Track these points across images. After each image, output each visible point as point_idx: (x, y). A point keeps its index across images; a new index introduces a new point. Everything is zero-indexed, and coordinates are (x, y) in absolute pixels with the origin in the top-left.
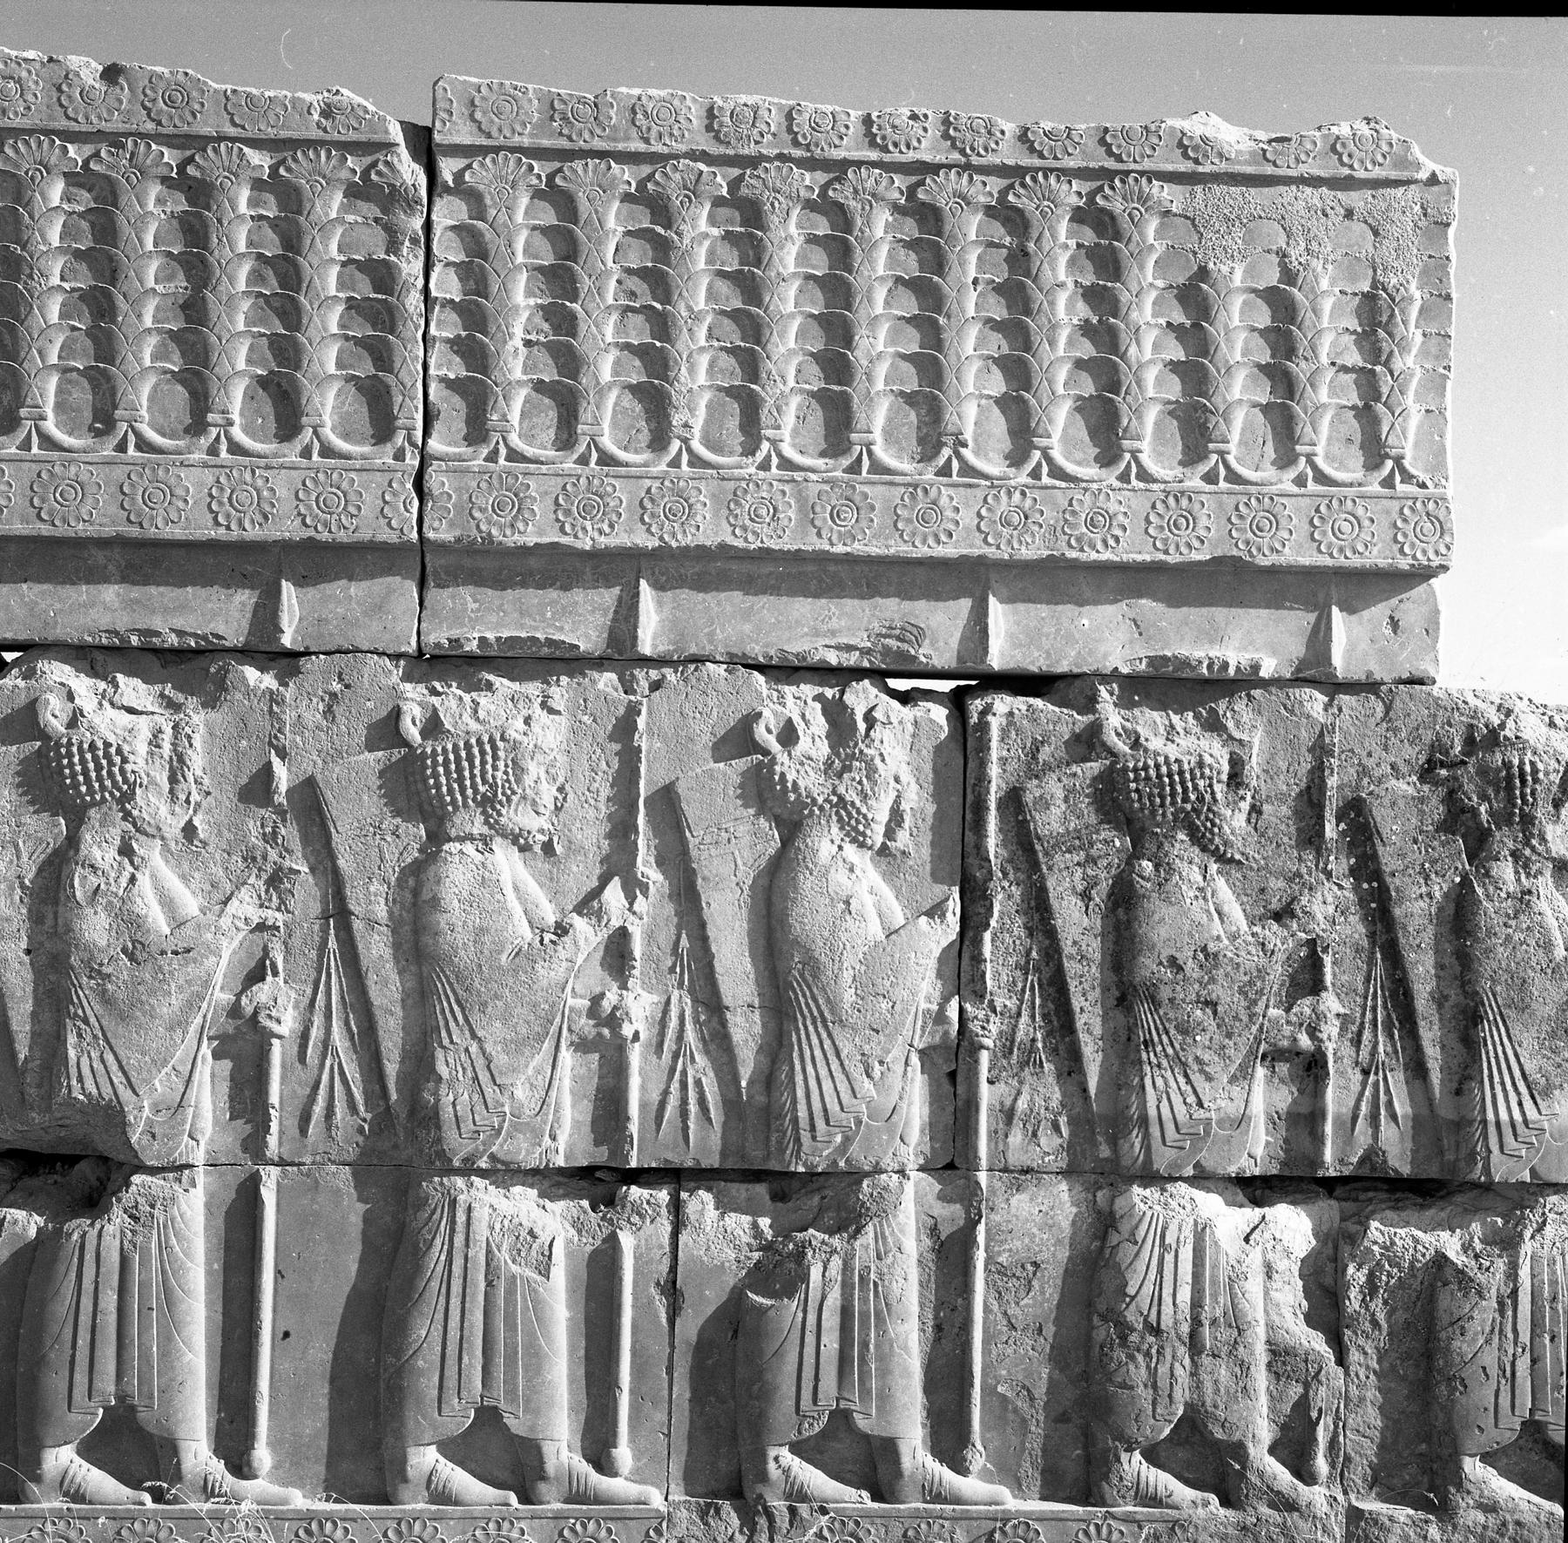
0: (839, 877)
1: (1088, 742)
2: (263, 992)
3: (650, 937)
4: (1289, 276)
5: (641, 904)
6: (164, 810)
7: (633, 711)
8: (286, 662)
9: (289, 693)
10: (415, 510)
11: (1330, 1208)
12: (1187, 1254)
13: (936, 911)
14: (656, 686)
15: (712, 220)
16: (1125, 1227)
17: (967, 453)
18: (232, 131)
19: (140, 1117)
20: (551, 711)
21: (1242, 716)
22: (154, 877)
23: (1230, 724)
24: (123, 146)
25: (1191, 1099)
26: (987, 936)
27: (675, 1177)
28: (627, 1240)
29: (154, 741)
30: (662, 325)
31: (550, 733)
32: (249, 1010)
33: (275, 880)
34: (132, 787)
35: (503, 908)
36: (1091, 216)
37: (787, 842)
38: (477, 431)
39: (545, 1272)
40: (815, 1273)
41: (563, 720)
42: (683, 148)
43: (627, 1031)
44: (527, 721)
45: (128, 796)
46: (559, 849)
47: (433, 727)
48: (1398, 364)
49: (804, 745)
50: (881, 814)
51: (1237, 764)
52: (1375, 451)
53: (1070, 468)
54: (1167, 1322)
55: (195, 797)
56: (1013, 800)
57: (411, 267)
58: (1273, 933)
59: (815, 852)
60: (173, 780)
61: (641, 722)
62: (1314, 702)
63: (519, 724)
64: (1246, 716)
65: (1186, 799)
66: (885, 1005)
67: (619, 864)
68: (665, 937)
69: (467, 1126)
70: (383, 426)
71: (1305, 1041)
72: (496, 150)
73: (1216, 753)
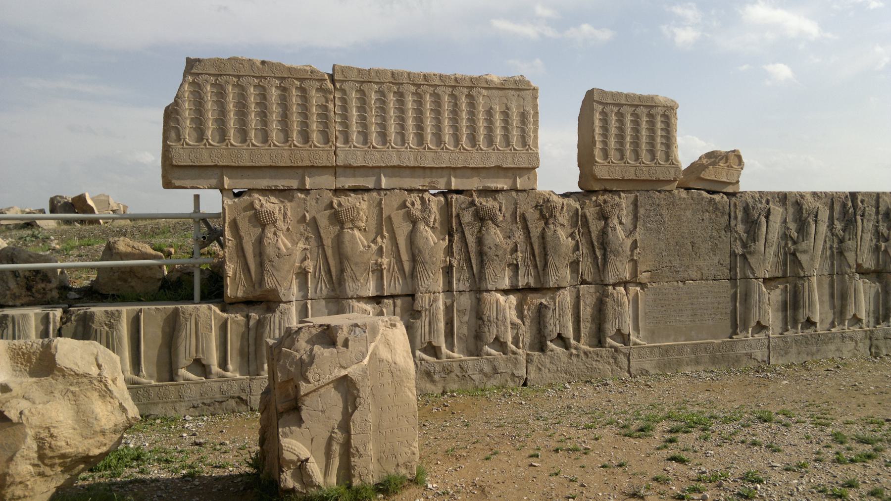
0: (424, 233)
1: (472, 203)
2: (306, 263)
3: (386, 247)
4: (508, 109)
6: (282, 225)
7: (381, 200)
8: (307, 191)
9: (308, 198)
11: (519, 295)
12: (495, 305)
14: (385, 195)
15: (394, 96)
16: (483, 301)
18: (291, 76)
19: (282, 292)
21: (500, 197)
22: (282, 240)
24: (266, 79)
27: (392, 297)
29: (280, 210)
30: (384, 119)
31: (364, 206)
33: (307, 239)
34: (276, 220)
35: (357, 242)
36: (469, 96)
37: (414, 226)
38: (347, 141)
40: (423, 315)
42: (387, 81)
43: (383, 267)
44: (360, 203)
45: (275, 222)
47: (340, 205)
48: (529, 126)
49: (416, 206)
51: (500, 207)
52: (524, 144)
53: (467, 148)
54: (492, 319)
55: (289, 222)
56: (458, 216)
57: (331, 106)
58: (508, 241)
60: (284, 218)
62: (514, 194)
63: (358, 204)
64: (501, 197)
66: (435, 259)
67: (379, 232)
68: (389, 247)
69: (352, 289)
70: (327, 141)
71: (515, 262)
72: (348, 81)
73: (497, 206)
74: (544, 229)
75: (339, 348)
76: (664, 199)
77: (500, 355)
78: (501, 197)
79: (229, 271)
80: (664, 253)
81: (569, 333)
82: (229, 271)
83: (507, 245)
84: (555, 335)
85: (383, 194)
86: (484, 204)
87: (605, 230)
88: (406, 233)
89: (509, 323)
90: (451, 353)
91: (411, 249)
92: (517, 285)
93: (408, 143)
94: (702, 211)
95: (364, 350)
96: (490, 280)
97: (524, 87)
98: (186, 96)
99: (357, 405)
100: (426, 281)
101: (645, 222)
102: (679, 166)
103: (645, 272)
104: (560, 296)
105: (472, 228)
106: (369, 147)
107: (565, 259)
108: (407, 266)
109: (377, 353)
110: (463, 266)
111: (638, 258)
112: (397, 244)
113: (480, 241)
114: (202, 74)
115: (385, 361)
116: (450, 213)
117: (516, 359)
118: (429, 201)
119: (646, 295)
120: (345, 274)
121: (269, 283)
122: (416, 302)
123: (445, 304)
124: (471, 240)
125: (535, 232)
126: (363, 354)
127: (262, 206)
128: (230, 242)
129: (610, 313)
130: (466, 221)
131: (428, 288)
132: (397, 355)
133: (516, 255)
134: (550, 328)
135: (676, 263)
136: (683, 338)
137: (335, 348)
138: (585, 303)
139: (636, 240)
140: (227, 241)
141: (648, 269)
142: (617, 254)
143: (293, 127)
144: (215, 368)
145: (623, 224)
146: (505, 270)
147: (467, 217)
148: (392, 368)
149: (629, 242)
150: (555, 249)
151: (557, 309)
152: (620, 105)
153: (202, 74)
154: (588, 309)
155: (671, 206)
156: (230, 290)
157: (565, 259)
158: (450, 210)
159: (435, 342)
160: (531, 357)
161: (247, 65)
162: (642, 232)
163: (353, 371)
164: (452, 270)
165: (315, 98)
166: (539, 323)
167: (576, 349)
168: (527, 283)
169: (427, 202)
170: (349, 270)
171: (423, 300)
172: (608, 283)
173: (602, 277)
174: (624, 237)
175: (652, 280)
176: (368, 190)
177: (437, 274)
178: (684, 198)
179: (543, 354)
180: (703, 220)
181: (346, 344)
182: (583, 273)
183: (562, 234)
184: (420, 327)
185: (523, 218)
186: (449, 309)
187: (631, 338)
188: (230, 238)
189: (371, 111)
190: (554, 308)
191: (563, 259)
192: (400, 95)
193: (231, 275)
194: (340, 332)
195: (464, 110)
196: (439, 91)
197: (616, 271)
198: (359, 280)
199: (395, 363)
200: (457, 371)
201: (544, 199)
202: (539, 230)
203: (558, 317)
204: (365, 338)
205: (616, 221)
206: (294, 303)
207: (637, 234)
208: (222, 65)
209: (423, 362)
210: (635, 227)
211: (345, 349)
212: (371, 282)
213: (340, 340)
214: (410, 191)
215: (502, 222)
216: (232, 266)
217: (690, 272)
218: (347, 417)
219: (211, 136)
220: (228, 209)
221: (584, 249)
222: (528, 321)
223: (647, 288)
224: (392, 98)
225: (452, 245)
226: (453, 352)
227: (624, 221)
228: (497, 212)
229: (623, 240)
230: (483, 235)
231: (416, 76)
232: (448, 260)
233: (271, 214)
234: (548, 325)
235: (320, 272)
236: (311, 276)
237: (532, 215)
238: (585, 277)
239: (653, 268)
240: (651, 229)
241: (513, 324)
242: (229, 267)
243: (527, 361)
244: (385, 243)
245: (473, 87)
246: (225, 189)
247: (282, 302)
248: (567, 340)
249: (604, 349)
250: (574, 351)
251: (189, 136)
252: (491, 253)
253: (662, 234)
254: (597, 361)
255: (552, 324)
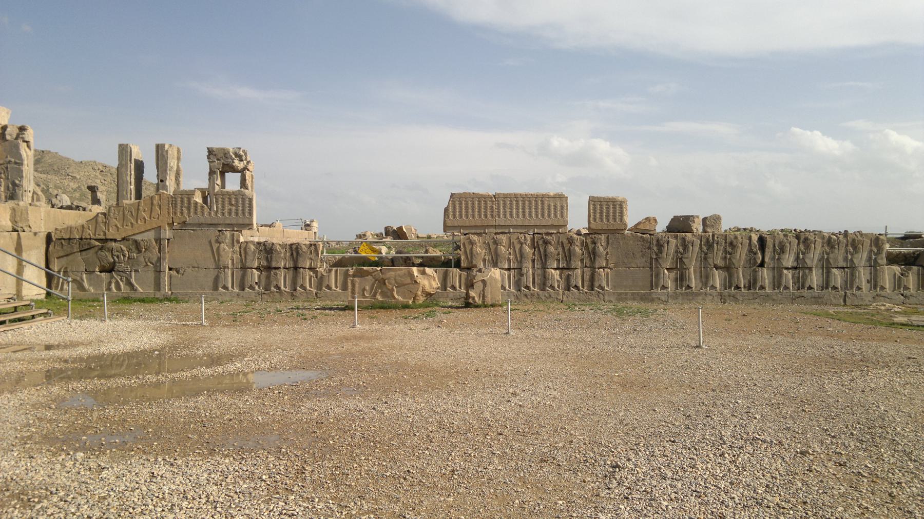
1: (543, 238)
4: (556, 204)
8: (486, 234)
11: (561, 270)
21: (553, 235)
27: (514, 269)
30: (512, 209)
31: (505, 238)
33: (486, 249)
36: (542, 201)
38: (499, 217)
47: (496, 238)
52: (562, 216)
56: (537, 242)
57: (494, 206)
62: (559, 234)
67: (510, 247)
70: (493, 217)
73: (552, 238)
74: (570, 248)
81: (580, 285)
84: (574, 285)
88: (518, 248)
108: (519, 259)
113: (545, 251)
121: (474, 262)
123: (532, 272)
124: (542, 250)
125: (567, 248)
129: (596, 278)
144: (458, 288)
147: (541, 242)
154: (588, 277)
163: (485, 278)
165: (489, 203)
171: (524, 271)
176: (506, 233)
181: (484, 272)
183: (577, 249)
185: (562, 242)
186: (534, 274)
192: (517, 201)
196: (531, 199)
202: (568, 247)
205: (599, 245)
213: (483, 271)
214: (521, 233)
218: (484, 288)
221: (586, 255)
222: (563, 280)
233: (475, 241)
237: (565, 241)
241: (558, 281)
244: (511, 251)
250: (581, 292)
251: (451, 217)
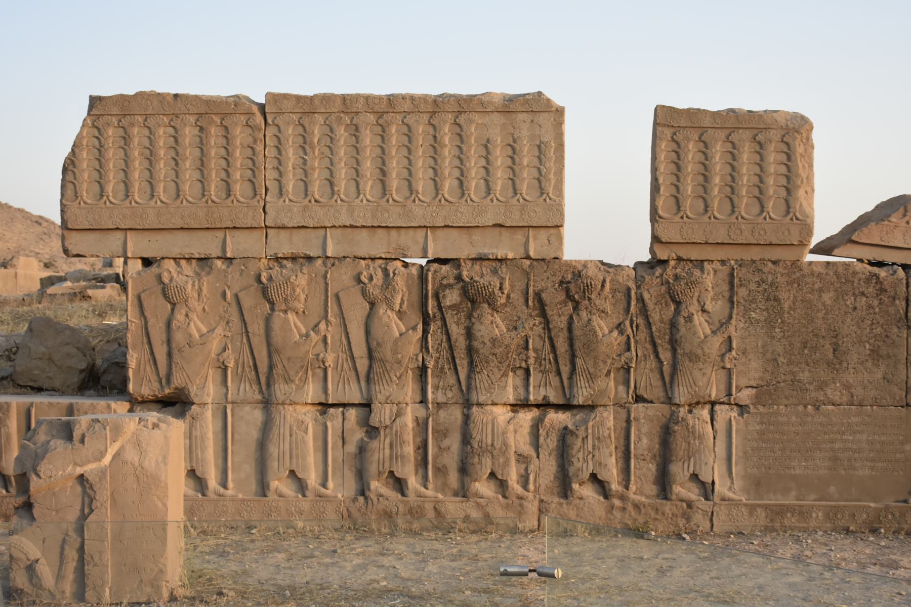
0: (385, 319)
2: (225, 355)
3: (332, 337)
5: (330, 328)
6: (196, 304)
7: (327, 272)
9: (230, 270)
10: (263, 218)
12: (490, 426)
13: (414, 328)
14: (333, 265)
15: (345, 131)
16: (472, 418)
17: (420, 196)
18: (209, 112)
19: (193, 391)
20: (303, 273)
22: (195, 324)
23: (500, 272)
24: (179, 117)
25: (490, 382)
26: (429, 335)
28: (329, 424)
29: (193, 285)
32: (222, 360)
34: (188, 298)
35: (291, 330)
37: (371, 309)
39: (306, 433)
40: (382, 433)
41: (306, 276)
42: (336, 110)
43: (327, 365)
44: (296, 276)
45: (186, 301)
46: (306, 313)
47: (270, 279)
48: (547, 165)
49: (375, 281)
50: (398, 301)
51: (501, 284)
53: (450, 199)
54: (484, 445)
55: (205, 300)
58: (513, 334)
59: (379, 312)
60: (199, 295)
61: (329, 276)
63: (294, 277)
64: (504, 270)
65: (486, 295)
66: (400, 356)
68: (337, 337)
69: (283, 392)
71: (524, 365)
72: (283, 113)
74: (571, 317)
75: (75, 445)
76: (782, 275)
77: (497, 498)
78: (504, 270)
79: (132, 362)
80: (781, 360)
81: (612, 473)
82: (132, 362)
83: (514, 340)
84: (586, 475)
85: (329, 265)
86: (477, 279)
87: (674, 321)
89: (512, 453)
90: (423, 489)
91: (367, 341)
92: (527, 399)
93: (364, 195)
94: (854, 294)
95: (103, 448)
96: (483, 389)
97: (540, 109)
98: (85, 143)
99: (93, 508)
100: (386, 386)
101: (746, 310)
102: (809, 221)
103: (747, 387)
104: (595, 418)
105: (456, 314)
106: (310, 201)
107: (605, 362)
109: (121, 454)
110: (442, 368)
111: (733, 366)
112: (348, 333)
113: (469, 334)
114: (103, 115)
115: (129, 463)
116: (424, 292)
117: (521, 505)
118: (394, 274)
119: (747, 424)
120: (274, 371)
121: (178, 380)
122: (373, 415)
123: (417, 420)
124: (457, 331)
125: (559, 322)
126: (101, 453)
127: (171, 280)
128: (133, 324)
129: (679, 445)
130: (448, 303)
131: (389, 397)
132: (147, 459)
133: (526, 355)
134: (577, 464)
135: (804, 376)
136: (813, 497)
137: (71, 443)
138: (639, 430)
139: (730, 337)
140: (129, 323)
141: (753, 383)
142: (694, 358)
143: (211, 177)
145: (709, 313)
146: (507, 375)
147: (452, 297)
148: (137, 472)
149: (716, 343)
150: (588, 348)
151: (590, 437)
152: (704, 130)
153: (103, 115)
154: (645, 441)
155: (796, 285)
156: (133, 386)
157: (605, 362)
158: (424, 286)
159: (398, 472)
160: (546, 505)
161: (155, 103)
162: (742, 325)
163: (89, 469)
164: (426, 372)
165: (240, 135)
166: (562, 456)
167: (622, 498)
168: (545, 397)
169: (391, 275)
170: (280, 366)
171: (381, 414)
172: (678, 402)
173: (669, 393)
174: (708, 332)
175: (758, 400)
177: (403, 378)
178: (820, 273)
179: (567, 504)
180: (855, 308)
181: (82, 441)
182: (638, 386)
183: (601, 326)
184: (377, 450)
186: (422, 425)
187: (717, 487)
188: (133, 320)
189: (314, 153)
190: (584, 436)
191: (601, 364)
192: (355, 131)
193: (133, 367)
194: (77, 427)
195: (446, 146)
197: (692, 384)
198: (292, 381)
199: (142, 468)
200: (431, 514)
201: (573, 272)
202: (564, 319)
203: (590, 449)
204: (104, 436)
205: (694, 308)
206: (210, 406)
207: (732, 328)
208: (126, 104)
209: (381, 499)
210: (730, 317)
211: (81, 445)
212: (311, 384)
213: (77, 434)
215: (505, 305)
216: (135, 355)
217: (829, 392)
218: (84, 517)
219: (112, 192)
220: (132, 283)
221: (639, 348)
223: (749, 412)
224: (342, 134)
225: (427, 337)
226: (426, 488)
227: (709, 307)
228: (496, 291)
229: (706, 337)
230: (473, 324)
231: (377, 101)
232: (420, 359)
234: (575, 460)
235: (243, 368)
236: (232, 372)
237: (554, 297)
238: (641, 392)
239: (761, 383)
240: (758, 322)
242: (132, 356)
243: (540, 510)
244: (333, 332)
245: (460, 112)
246: (128, 258)
247: (193, 403)
248: (606, 484)
249: (669, 503)
250: (617, 502)
251: (87, 192)
252: (484, 351)
253: (777, 330)
254: (655, 519)
255: (581, 459)
